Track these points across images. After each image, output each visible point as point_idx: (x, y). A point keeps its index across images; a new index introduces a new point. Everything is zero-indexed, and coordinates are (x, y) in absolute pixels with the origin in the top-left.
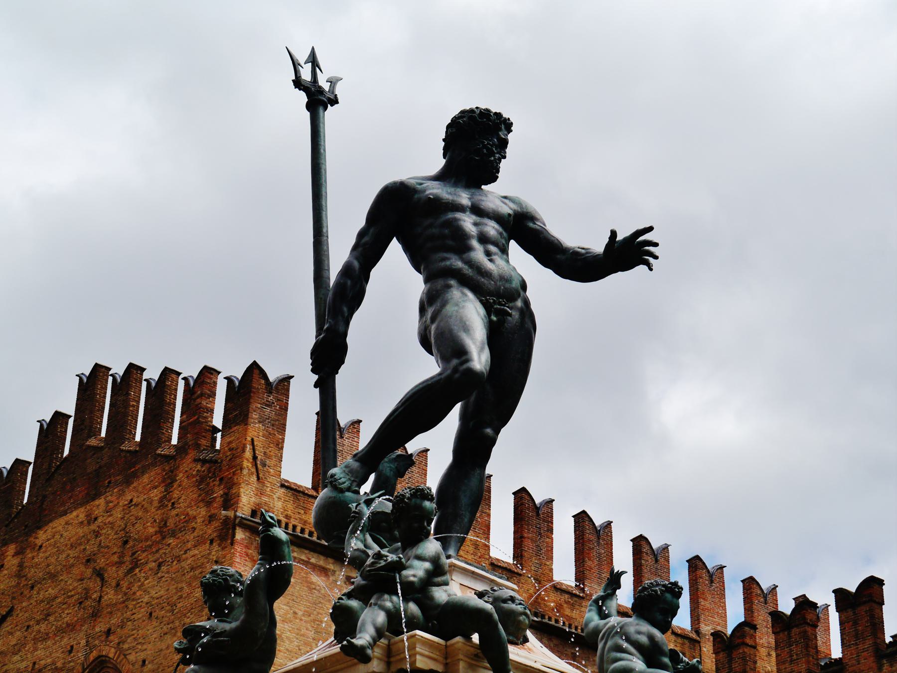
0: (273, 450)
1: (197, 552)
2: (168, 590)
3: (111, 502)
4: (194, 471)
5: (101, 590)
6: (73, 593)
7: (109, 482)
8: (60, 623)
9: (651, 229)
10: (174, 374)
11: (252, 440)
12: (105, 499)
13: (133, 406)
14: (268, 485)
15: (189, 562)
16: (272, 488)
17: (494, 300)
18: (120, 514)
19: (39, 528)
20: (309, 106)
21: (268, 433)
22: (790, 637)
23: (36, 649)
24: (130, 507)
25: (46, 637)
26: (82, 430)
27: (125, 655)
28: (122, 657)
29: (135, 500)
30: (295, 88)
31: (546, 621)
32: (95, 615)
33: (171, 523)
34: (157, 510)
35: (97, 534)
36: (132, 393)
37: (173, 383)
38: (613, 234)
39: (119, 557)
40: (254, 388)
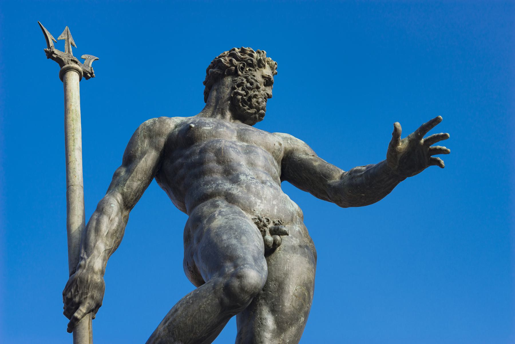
17: (268, 220)
30: (48, 58)
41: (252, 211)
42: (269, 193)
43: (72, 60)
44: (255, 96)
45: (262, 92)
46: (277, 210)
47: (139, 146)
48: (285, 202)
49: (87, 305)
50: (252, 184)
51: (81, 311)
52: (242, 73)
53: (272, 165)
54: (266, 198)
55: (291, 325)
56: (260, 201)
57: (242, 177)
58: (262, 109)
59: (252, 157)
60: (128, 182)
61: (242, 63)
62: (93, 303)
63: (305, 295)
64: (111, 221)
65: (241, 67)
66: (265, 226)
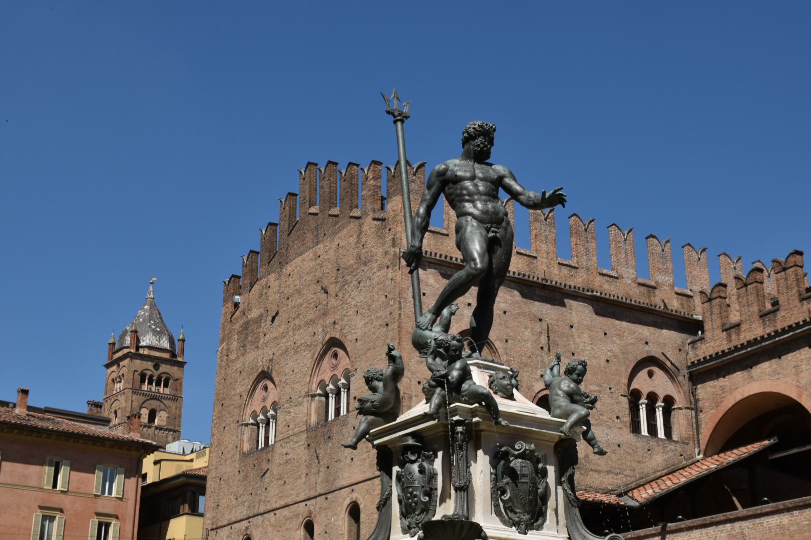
1: (380, 274)
2: (365, 297)
3: (327, 246)
6: (311, 301)
7: (325, 234)
8: (306, 319)
9: (561, 189)
12: (323, 244)
13: (333, 187)
15: (376, 280)
19: (287, 263)
20: (395, 122)
22: (747, 291)
23: (294, 335)
25: (300, 327)
26: (305, 203)
27: (345, 336)
28: (344, 337)
29: (340, 244)
31: (595, 293)
32: (325, 314)
33: (363, 257)
35: (321, 266)
38: (544, 193)
39: (335, 279)
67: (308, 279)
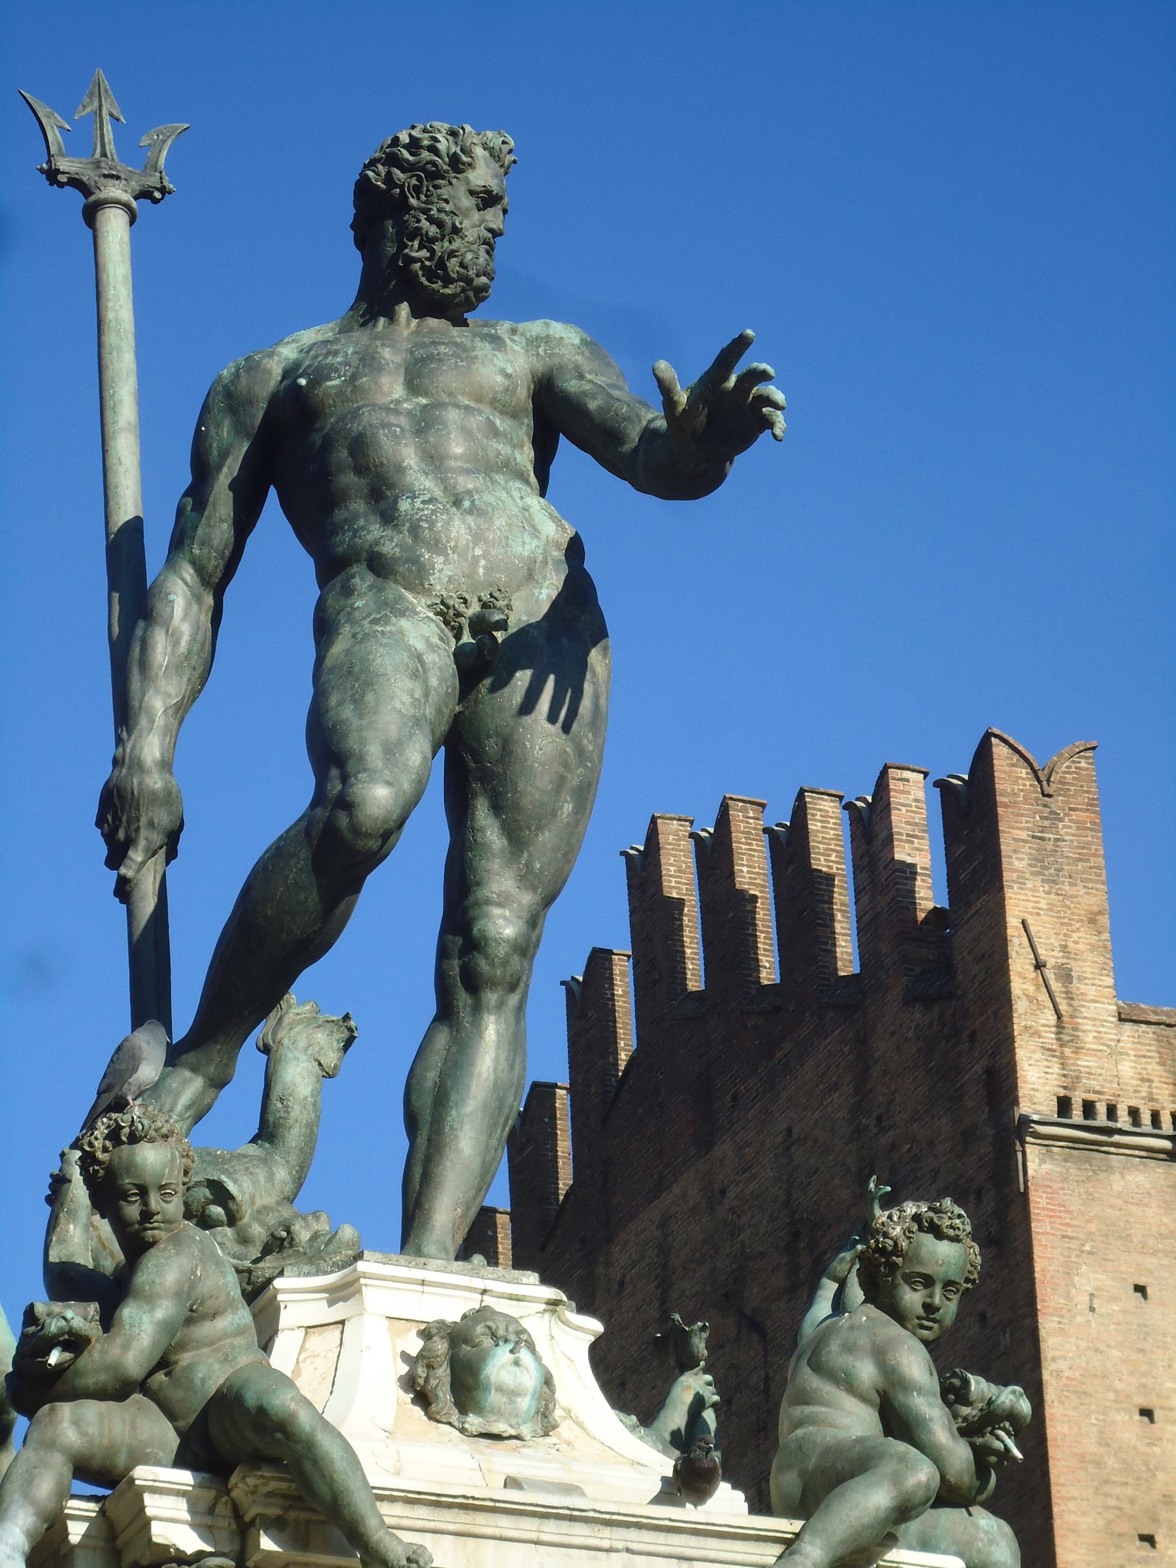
0: (1082, 939)
3: (747, 1145)
4: (909, 1029)
5: (766, 1362)
7: (735, 1097)
10: (823, 799)
11: (1024, 923)
14: (1087, 1027)
16: (1099, 1032)
17: (465, 601)
18: (771, 1170)
21: (1060, 898)
24: (788, 1149)
30: (51, 184)
34: (847, 1144)
36: (745, 869)
37: (829, 823)
40: (1005, 794)
41: (426, 586)
42: (463, 531)
43: (105, 176)
44: (452, 254)
45: (471, 234)
46: (485, 567)
47: (212, 438)
48: (507, 538)
49: (142, 843)
50: (422, 520)
51: (131, 859)
52: (418, 199)
53: (487, 437)
54: (456, 547)
55: (539, 828)
56: (441, 559)
57: (404, 505)
58: (478, 275)
59: (432, 439)
60: (200, 531)
61: (414, 176)
62: (155, 836)
63: (566, 752)
64: (173, 635)
65: (415, 186)
66: (458, 614)
67: (687, 1293)
